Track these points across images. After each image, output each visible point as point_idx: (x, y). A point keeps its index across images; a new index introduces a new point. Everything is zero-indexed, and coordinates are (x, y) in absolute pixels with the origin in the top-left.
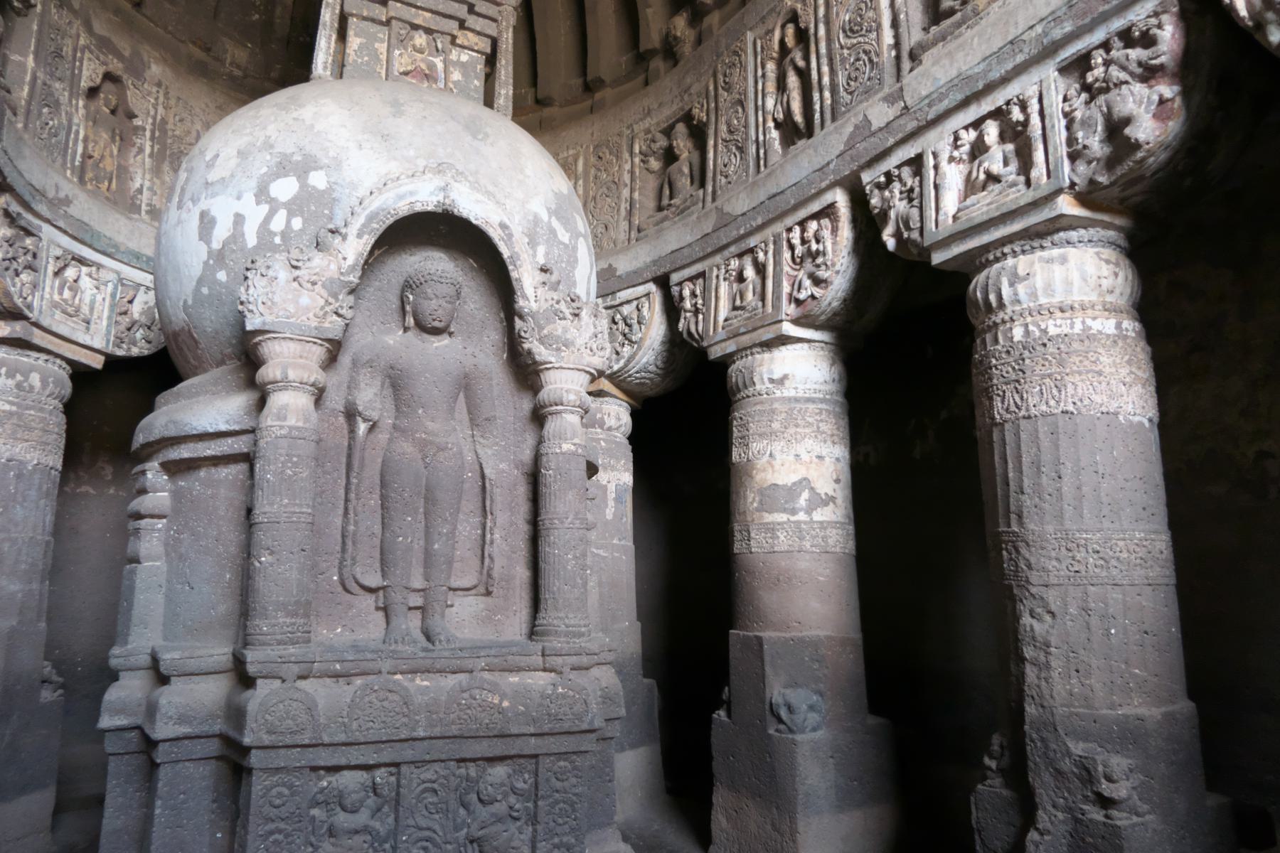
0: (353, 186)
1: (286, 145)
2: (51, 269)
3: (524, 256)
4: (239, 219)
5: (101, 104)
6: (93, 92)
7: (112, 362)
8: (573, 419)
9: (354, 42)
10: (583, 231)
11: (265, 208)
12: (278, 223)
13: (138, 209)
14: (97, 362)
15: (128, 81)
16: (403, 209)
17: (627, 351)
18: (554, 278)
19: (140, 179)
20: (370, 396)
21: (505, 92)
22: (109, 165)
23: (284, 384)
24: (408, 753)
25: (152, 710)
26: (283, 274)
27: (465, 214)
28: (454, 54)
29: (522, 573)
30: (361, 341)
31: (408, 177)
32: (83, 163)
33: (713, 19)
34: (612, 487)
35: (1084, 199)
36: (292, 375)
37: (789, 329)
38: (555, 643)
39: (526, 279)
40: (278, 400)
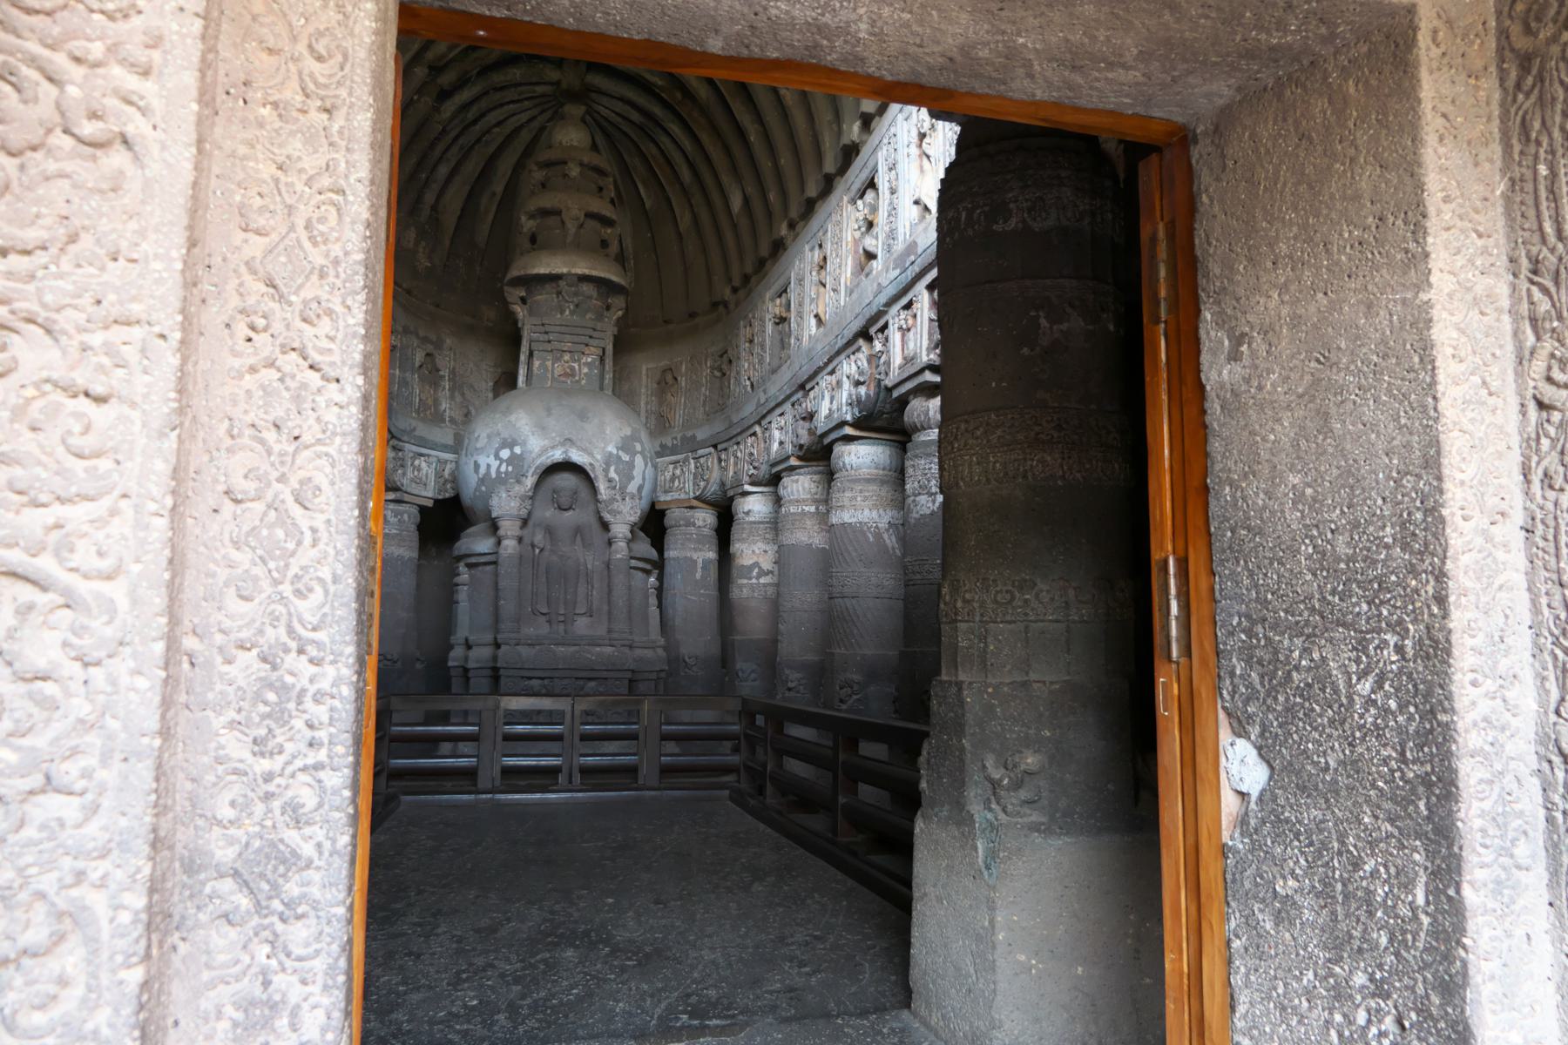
1: (505, 434)
4: (489, 466)
7: (436, 501)
8: (623, 544)
9: (537, 363)
12: (503, 468)
13: (443, 421)
14: (430, 504)
16: (549, 462)
17: (702, 484)
19: (444, 405)
20: (539, 538)
21: (609, 376)
22: (430, 402)
23: (507, 537)
24: (556, 674)
25: (466, 659)
29: (605, 608)
30: (537, 514)
31: (553, 448)
33: (741, 293)
34: (700, 561)
35: (799, 458)
37: (748, 488)
38: (615, 635)
39: (602, 486)
40: (505, 543)
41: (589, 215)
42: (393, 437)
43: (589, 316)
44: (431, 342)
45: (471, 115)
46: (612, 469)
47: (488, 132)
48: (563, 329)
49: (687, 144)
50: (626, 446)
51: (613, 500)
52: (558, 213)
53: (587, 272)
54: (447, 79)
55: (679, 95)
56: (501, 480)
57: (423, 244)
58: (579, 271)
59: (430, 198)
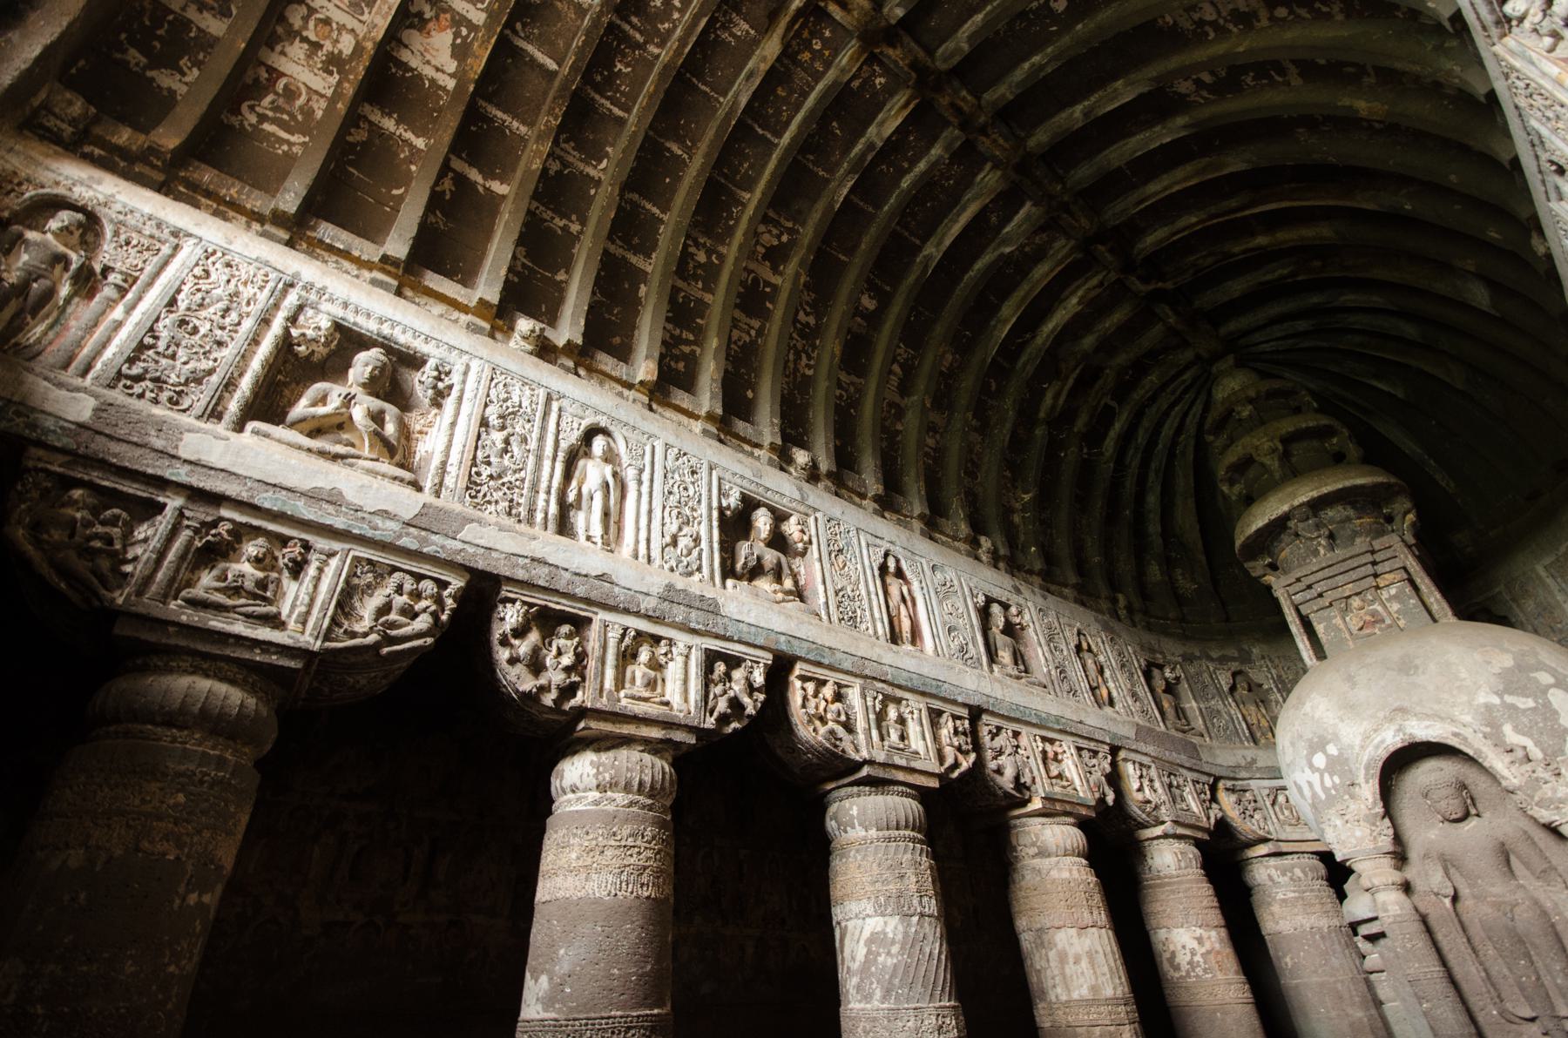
0: (1351, 747)
2: (1268, 804)
3: (1484, 749)
5: (1242, 691)
6: (1233, 689)
9: (1320, 629)
10: (1552, 680)
11: (1317, 775)
12: (1328, 783)
15: (1246, 668)
18: (1520, 754)
21: (1435, 598)
22: (1264, 723)
26: (1339, 822)
27: (1424, 739)
28: (1385, 595)
32: (1251, 733)
36: (1376, 882)
39: (1497, 762)
40: (1382, 897)
41: (1287, 440)
42: (1217, 779)
43: (1358, 540)
44: (1234, 659)
45: (1141, 438)
46: (1507, 729)
47: (1174, 443)
48: (1327, 573)
49: (1377, 300)
50: (1512, 682)
51: (1535, 783)
52: (1247, 462)
53: (1315, 494)
54: (1080, 424)
55: (1317, 263)
56: (1331, 800)
57: (1179, 571)
58: (1304, 499)
59: (1154, 528)
